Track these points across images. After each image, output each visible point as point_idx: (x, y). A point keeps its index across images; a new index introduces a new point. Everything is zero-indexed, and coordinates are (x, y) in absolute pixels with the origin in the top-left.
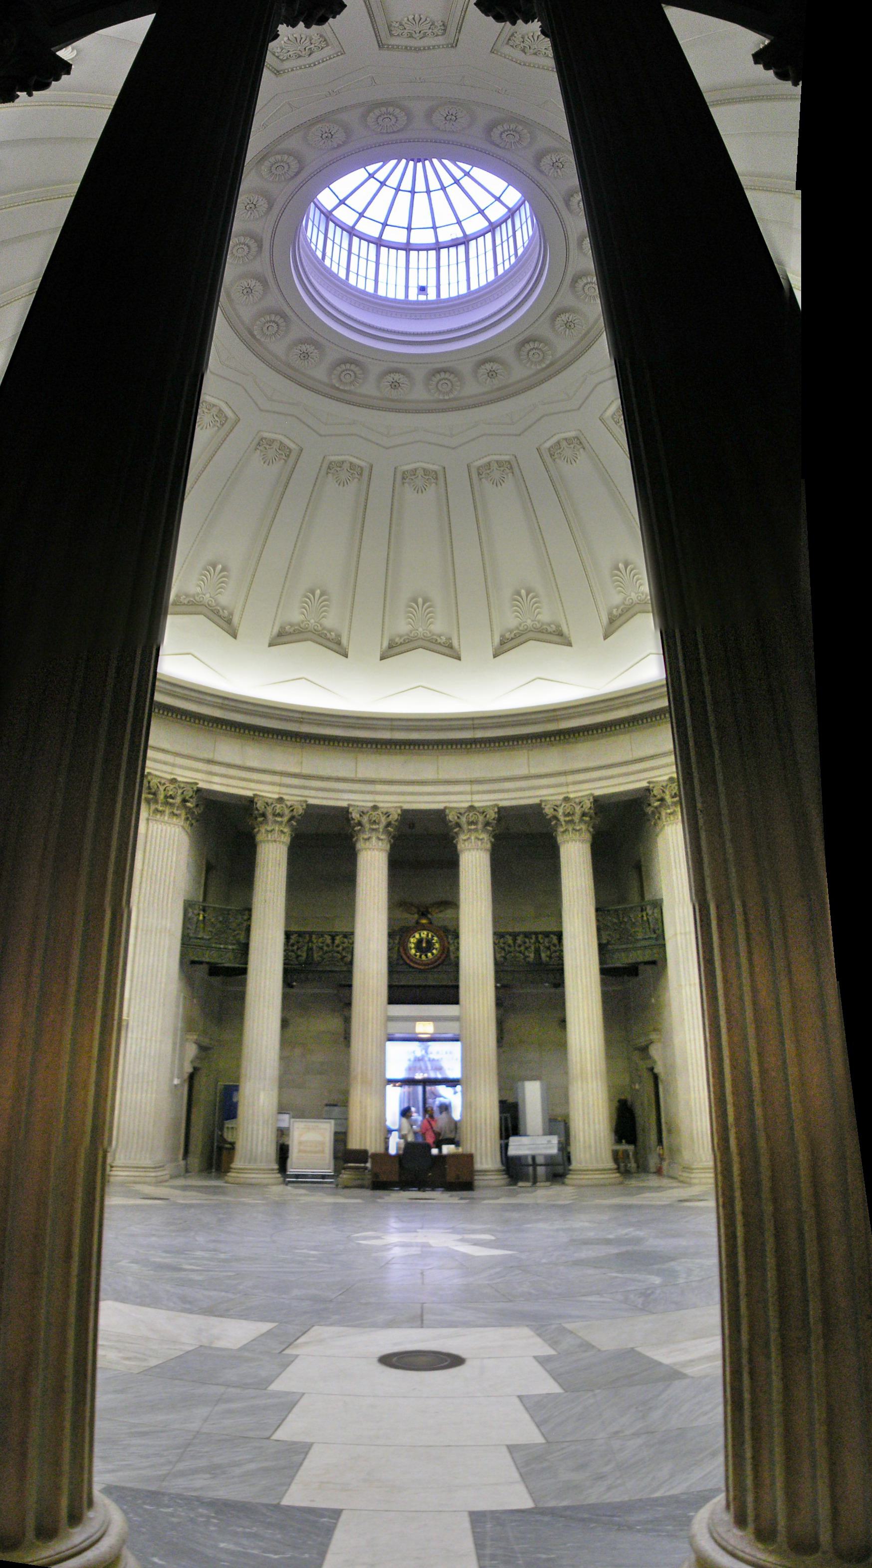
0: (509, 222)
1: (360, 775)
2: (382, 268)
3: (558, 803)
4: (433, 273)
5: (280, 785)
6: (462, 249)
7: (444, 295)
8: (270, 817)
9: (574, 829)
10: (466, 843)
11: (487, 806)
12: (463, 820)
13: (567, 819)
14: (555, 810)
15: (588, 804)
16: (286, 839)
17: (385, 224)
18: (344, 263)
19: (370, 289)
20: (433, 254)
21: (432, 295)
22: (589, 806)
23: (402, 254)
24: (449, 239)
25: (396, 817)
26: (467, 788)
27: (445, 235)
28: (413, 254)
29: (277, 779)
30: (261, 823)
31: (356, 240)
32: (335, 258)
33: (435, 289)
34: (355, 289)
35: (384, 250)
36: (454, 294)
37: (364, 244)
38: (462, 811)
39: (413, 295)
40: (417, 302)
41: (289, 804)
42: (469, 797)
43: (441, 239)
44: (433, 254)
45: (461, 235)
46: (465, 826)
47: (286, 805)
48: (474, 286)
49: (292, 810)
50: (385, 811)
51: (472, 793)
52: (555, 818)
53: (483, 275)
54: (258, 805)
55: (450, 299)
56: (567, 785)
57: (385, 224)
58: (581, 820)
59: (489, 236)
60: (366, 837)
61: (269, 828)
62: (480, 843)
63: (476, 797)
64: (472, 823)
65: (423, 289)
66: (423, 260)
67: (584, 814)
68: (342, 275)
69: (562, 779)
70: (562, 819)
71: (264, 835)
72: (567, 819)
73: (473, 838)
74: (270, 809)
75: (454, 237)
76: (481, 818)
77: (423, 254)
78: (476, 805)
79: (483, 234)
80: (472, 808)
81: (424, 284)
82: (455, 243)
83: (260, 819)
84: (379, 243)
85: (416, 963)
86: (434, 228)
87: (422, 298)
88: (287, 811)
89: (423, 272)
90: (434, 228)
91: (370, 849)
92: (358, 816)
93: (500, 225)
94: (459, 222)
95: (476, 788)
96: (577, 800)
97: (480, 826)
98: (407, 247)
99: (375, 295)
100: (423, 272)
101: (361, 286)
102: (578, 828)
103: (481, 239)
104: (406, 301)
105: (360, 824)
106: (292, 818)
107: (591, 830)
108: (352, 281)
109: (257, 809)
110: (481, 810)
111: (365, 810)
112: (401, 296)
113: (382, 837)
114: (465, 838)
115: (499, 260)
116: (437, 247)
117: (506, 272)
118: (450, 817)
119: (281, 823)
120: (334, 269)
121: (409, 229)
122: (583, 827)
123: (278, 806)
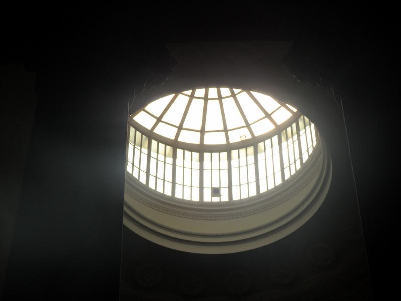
0: (294, 125)
2: (179, 170)
4: (225, 173)
6: (251, 150)
7: (236, 197)
17: (180, 128)
18: (144, 167)
19: (168, 192)
20: (224, 155)
21: (224, 198)
23: (196, 155)
24: (239, 140)
27: (234, 138)
28: (206, 155)
31: (154, 143)
32: (137, 163)
33: (227, 189)
34: (155, 192)
35: (180, 152)
36: (245, 196)
37: (162, 146)
39: (208, 198)
40: (212, 204)
43: (231, 141)
44: (224, 155)
45: (249, 137)
48: (263, 190)
53: (271, 181)
55: (241, 201)
57: (180, 128)
59: (275, 139)
65: (216, 192)
66: (215, 162)
68: (143, 180)
75: (243, 139)
77: (215, 155)
79: (269, 136)
81: (216, 185)
82: (243, 145)
84: (175, 145)
86: (225, 130)
87: (216, 199)
89: (215, 174)
90: (225, 130)
93: (285, 129)
94: (248, 126)
98: (201, 149)
99: (173, 198)
100: (215, 174)
101: (160, 190)
103: (268, 142)
104: (201, 203)
108: (152, 186)
112: (196, 198)
115: (286, 164)
116: (228, 148)
117: (292, 177)
120: (136, 175)
121: (203, 132)
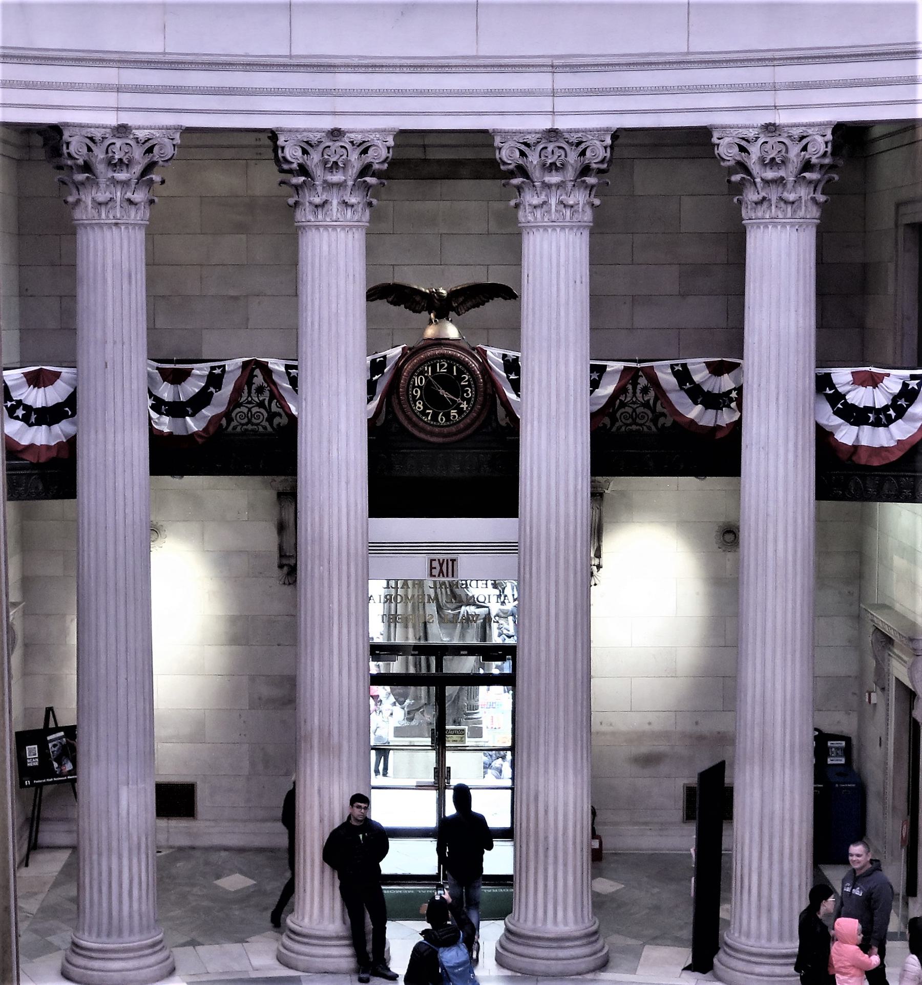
1: (300, 49)
3: (751, 134)
5: (119, 89)
8: (100, 168)
9: (781, 199)
10: (538, 213)
11: (585, 131)
12: (533, 158)
13: (770, 174)
14: (742, 149)
15: (820, 145)
16: (139, 215)
22: (822, 149)
25: (384, 153)
26: (543, 81)
29: (110, 75)
30: (78, 186)
38: (531, 139)
41: (142, 134)
42: (546, 104)
46: (536, 174)
47: (137, 140)
49: (150, 150)
50: (358, 138)
51: (554, 93)
52: (742, 167)
54: (72, 149)
56: (775, 88)
58: (799, 179)
60: (317, 200)
61: (102, 197)
62: (568, 212)
63: (563, 104)
64: (553, 167)
67: (807, 166)
69: (762, 74)
70: (755, 169)
71: (92, 212)
72: (770, 174)
73: (553, 202)
74: (99, 153)
76: (573, 157)
78: (562, 124)
80: (553, 134)
83: (81, 177)
85: (422, 430)
88: (137, 153)
91: (326, 227)
92: (299, 153)
95: (565, 81)
96: (796, 132)
97: (570, 174)
102: (792, 197)
105: (303, 170)
106: (149, 168)
107: (822, 198)
109: (70, 156)
110: (574, 138)
111: (314, 138)
113: (353, 200)
114: (536, 201)
118: (504, 155)
119: (125, 184)
122: (803, 192)
123: (119, 143)
